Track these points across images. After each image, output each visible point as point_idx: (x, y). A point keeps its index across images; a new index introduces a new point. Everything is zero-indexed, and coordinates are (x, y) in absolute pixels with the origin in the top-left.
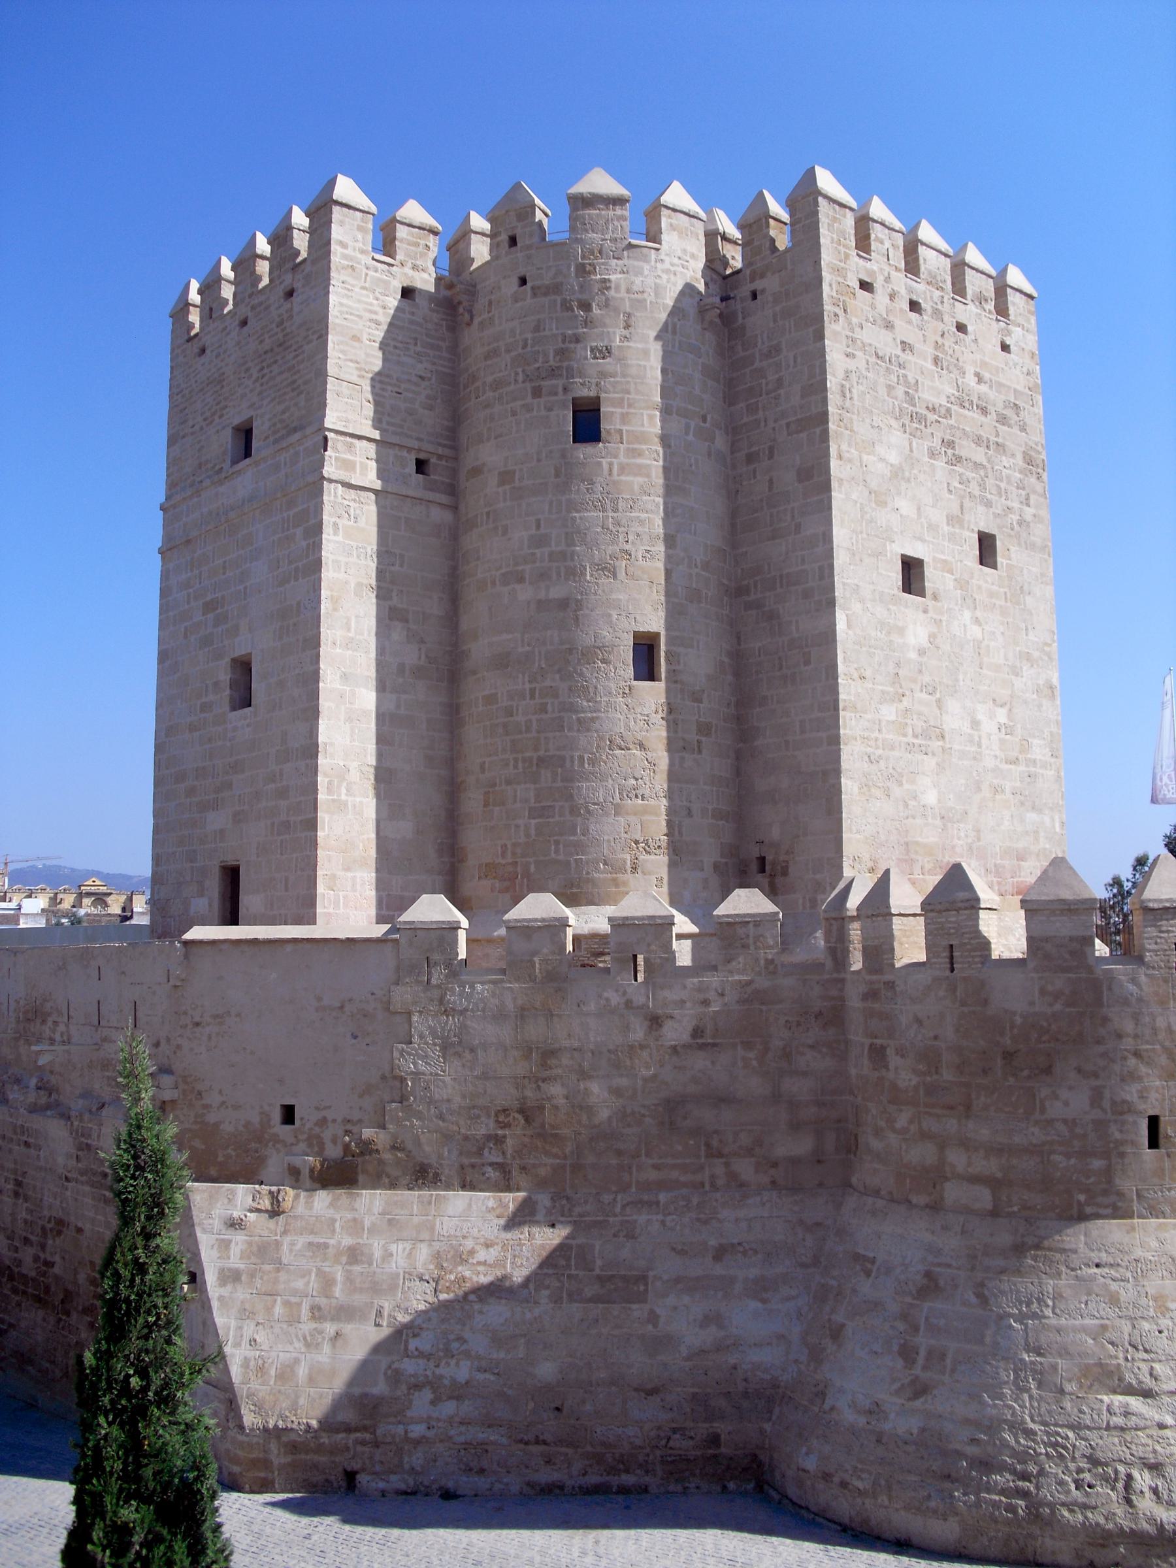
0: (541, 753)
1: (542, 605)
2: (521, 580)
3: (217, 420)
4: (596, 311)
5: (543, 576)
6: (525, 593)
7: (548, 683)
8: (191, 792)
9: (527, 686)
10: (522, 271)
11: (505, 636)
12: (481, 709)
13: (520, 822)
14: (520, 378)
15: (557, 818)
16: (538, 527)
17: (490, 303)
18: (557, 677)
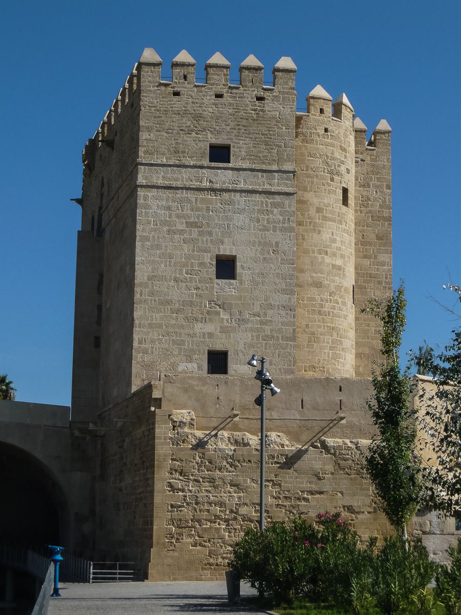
0: (334, 325)
1: (334, 266)
2: (326, 253)
3: (194, 134)
4: (347, 154)
5: (334, 255)
6: (328, 260)
7: (335, 298)
8: (178, 311)
9: (329, 297)
10: (327, 127)
11: (319, 275)
12: (305, 302)
13: (326, 351)
14: (326, 171)
15: (338, 352)
16: (333, 234)
17: (311, 133)
18: (338, 296)
